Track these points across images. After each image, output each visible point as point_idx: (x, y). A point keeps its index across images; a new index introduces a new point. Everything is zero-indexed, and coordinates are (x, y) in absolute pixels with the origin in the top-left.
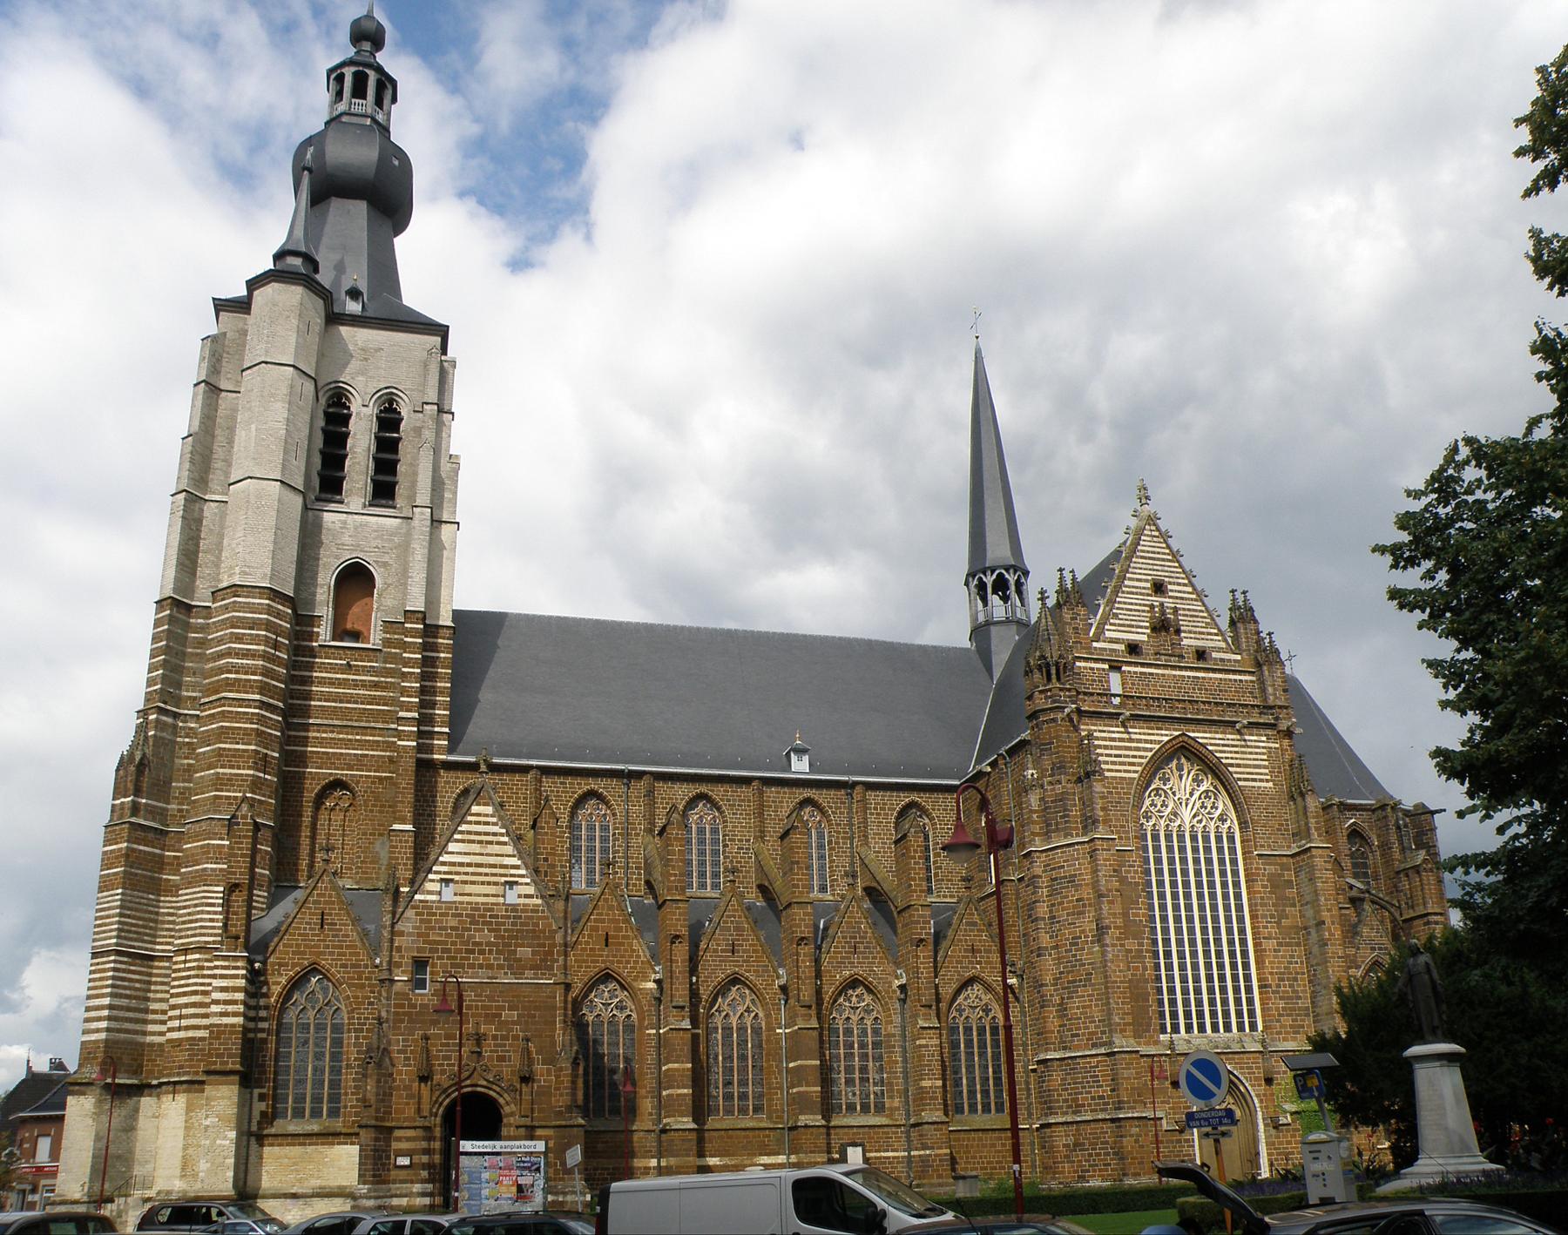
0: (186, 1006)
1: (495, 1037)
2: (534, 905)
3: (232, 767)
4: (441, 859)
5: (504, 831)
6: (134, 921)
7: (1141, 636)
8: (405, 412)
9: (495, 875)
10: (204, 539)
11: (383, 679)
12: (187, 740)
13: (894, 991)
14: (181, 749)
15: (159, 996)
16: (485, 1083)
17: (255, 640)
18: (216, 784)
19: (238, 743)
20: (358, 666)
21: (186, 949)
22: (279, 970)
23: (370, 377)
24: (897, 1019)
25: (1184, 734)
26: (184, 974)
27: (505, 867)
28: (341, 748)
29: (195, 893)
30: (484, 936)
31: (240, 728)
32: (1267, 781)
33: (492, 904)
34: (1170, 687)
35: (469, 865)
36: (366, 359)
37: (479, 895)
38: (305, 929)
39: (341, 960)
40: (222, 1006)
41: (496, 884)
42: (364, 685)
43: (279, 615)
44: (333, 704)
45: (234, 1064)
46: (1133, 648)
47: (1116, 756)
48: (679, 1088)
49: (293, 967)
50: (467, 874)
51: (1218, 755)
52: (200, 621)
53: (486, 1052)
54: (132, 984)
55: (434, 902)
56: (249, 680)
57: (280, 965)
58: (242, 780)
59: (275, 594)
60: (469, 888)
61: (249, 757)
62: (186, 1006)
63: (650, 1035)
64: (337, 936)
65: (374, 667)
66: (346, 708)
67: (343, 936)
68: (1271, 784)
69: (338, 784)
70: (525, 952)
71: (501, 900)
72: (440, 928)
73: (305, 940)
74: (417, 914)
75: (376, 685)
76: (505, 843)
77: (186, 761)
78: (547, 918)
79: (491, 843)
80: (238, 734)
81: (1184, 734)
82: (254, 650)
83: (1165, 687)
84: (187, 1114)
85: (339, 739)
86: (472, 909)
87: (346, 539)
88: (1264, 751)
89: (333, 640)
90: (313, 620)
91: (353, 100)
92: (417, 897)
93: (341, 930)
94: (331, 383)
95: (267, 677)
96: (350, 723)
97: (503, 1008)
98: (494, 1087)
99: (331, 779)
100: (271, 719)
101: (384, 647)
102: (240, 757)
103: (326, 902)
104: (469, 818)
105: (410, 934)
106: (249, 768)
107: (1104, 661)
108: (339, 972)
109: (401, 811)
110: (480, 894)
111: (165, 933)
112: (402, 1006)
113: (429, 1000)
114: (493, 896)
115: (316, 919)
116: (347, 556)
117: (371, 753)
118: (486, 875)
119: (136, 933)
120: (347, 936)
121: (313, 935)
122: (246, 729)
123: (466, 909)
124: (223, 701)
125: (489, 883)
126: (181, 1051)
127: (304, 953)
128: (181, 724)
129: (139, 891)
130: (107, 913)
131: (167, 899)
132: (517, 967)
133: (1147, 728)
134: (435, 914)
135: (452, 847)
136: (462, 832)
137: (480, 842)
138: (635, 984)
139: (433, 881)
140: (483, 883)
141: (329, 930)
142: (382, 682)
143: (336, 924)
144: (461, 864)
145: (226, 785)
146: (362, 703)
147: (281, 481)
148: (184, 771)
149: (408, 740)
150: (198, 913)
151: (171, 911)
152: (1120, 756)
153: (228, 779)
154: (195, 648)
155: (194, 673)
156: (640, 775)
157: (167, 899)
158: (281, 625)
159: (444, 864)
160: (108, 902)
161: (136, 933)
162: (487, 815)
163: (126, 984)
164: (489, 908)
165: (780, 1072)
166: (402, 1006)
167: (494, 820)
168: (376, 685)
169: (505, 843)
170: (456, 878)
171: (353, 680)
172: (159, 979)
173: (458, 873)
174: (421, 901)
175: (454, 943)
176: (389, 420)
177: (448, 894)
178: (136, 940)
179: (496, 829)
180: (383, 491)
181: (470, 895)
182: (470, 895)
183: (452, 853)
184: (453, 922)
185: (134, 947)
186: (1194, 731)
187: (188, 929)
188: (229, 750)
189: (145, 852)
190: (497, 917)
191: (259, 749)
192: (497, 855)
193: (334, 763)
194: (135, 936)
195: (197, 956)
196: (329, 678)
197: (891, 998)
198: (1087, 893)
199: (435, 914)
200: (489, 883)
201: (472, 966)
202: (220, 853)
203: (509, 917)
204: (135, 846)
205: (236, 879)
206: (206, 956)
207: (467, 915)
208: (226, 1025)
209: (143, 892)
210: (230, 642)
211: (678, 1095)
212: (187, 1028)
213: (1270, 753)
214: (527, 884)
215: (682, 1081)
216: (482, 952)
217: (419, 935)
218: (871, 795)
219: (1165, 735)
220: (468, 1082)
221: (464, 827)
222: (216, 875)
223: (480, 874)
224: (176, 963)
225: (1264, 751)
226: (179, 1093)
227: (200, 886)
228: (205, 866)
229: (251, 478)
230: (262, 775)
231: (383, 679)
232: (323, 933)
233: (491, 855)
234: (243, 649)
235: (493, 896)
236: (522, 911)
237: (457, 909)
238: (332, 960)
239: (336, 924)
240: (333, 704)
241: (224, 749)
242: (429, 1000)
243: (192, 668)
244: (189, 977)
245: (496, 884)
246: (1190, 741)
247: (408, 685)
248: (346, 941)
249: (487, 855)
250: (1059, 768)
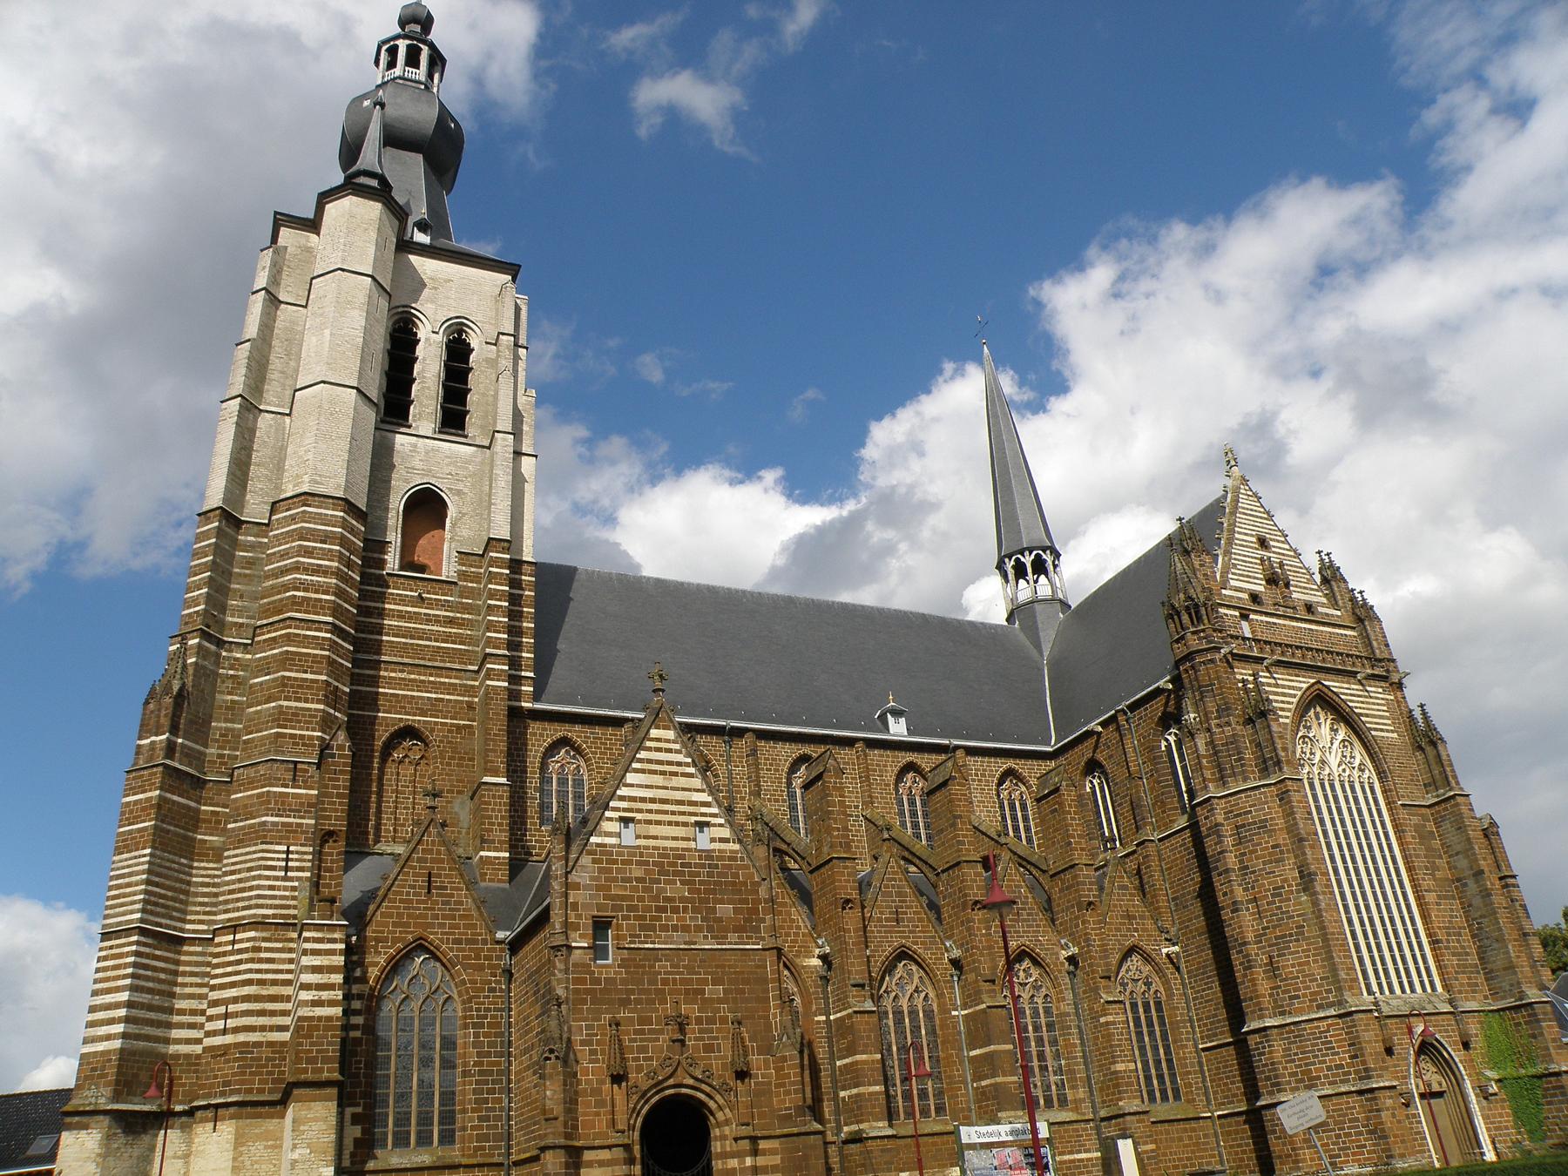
0: (235, 1000)
1: (699, 1021)
2: (731, 851)
3: (298, 700)
4: (619, 792)
5: (689, 760)
6: (163, 892)
7: (1260, 587)
8: (474, 341)
9: (683, 813)
10: (257, 451)
11: (459, 615)
12: (231, 672)
13: (1062, 964)
14: (223, 682)
15: (188, 990)
16: (691, 1082)
17: (327, 555)
18: (279, 719)
19: (306, 672)
20: (431, 599)
21: (235, 927)
22: (376, 947)
23: (440, 306)
24: (1069, 995)
25: (1318, 682)
26: (232, 958)
28: (413, 690)
29: (247, 854)
30: (676, 889)
31: (308, 655)
32: (1392, 731)
33: (683, 849)
35: (653, 801)
36: (436, 288)
37: (666, 838)
38: (408, 894)
39: (454, 934)
40: (314, 992)
41: (685, 824)
42: (437, 620)
43: (352, 530)
44: (403, 640)
45: (330, 1072)
46: (1255, 597)
48: (870, 1085)
49: (394, 943)
50: (650, 811)
51: (1350, 704)
52: (249, 538)
53: (690, 1040)
54: (155, 974)
55: (613, 846)
56: (320, 600)
57: (378, 940)
58: (310, 716)
59: (350, 507)
60: (654, 830)
61: (319, 689)
62: (235, 1000)
63: (819, 1022)
64: (448, 903)
65: (449, 601)
66: (417, 645)
67: (456, 903)
68: (1395, 735)
69: (409, 732)
70: (725, 910)
72: (624, 880)
73: (409, 908)
74: (594, 861)
75: (451, 622)
76: (690, 775)
77: (229, 697)
78: (747, 867)
79: (675, 774)
80: (306, 661)
82: (326, 566)
84: (235, 1149)
85: (410, 680)
86: (660, 855)
87: (417, 463)
88: (1383, 702)
90: (382, 546)
91: (407, 68)
92: (593, 839)
93: (452, 896)
94: (398, 307)
95: (339, 598)
96: (422, 662)
97: (705, 981)
98: (704, 1087)
99: (402, 725)
100: (342, 647)
101: (460, 580)
102: (308, 687)
103: (433, 861)
104: (648, 744)
105: (586, 887)
106: (319, 702)
107: (1235, 608)
108: (451, 950)
109: (492, 762)
110: (668, 836)
111: (198, 909)
112: (583, 981)
113: (615, 973)
114: (683, 839)
115: (421, 882)
116: (418, 480)
117: (448, 697)
118: (673, 813)
119: (163, 906)
120: (461, 903)
121: (418, 902)
122: (315, 656)
123: (652, 855)
124: (288, 623)
125: (677, 824)
126: (227, 1061)
127: (407, 925)
128: (224, 654)
129: (169, 853)
130: (127, 880)
131: (202, 865)
132: (717, 928)
134: (615, 862)
135: (631, 778)
136: (641, 761)
137: (663, 773)
138: (798, 961)
139: (610, 819)
140: (670, 823)
141: (438, 895)
142: (458, 618)
143: (446, 888)
144: (643, 800)
145: (291, 720)
146: (436, 641)
147: (357, 389)
148: (227, 708)
149: (498, 680)
150: (254, 878)
151: (207, 880)
153: (293, 714)
154: (243, 568)
155: (241, 597)
156: (740, 733)
157: (202, 865)
158: (354, 543)
159: (622, 798)
160: (129, 866)
161: (163, 906)
162: (668, 741)
163: (149, 973)
164: (679, 855)
165: (961, 1062)
166: (583, 981)
167: (677, 747)
168: (451, 622)
169: (690, 775)
170: (639, 816)
171: (425, 614)
172: (188, 969)
173: (639, 811)
174: (598, 845)
175: (641, 899)
176: (457, 351)
177: (629, 837)
178: (163, 916)
179: (680, 758)
180: (453, 419)
181: (655, 838)
182: (655, 838)
183: (632, 785)
184: (638, 872)
185: (160, 925)
187: (238, 900)
188: (296, 679)
189: (179, 803)
190: (689, 865)
191: (330, 680)
193: (404, 708)
194: (162, 910)
195: (252, 934)
196: (398, 611)
197: (1060, 971)
198: (1283, 838)
199: (615, 862)
200: (677, 824)
201: (665, 928)
202: (283, 803)
203: (703, 866)
204: (169, 795)
205: (329, 825)
206: (264, 934)
207: (655, 863)
208: (320, 1018)
209: (175, 854)
210: (297, 556)
211: (871, 1094)
212: (236, 1030)
213: (1388, 704)
214: (721, 825)
215: (872, 1076)
216: (675, 910)
217: (598, 888)
218: (970, 760)
219: (1303, 682)
220: (671, 1082)
221: (642, 755)
222: (278, 831)
223: (666, 812)
224: (220, 944)
225: (1383, 702)
226: (223, 1119)
227: (256, 844)
228: (264, 819)
229: (324, 382)
230: (332, 711)
231: (459, 615)
232: (430, 899)
233: (677, 789)
234: (313, 564)
235: (683, 839)
237: (641, 855)
238: (442, 934)
239: (446, 888)
240: (403, 640)
241: (289, 678)
242: (615, 973)
243: (239, 590)
244: (239, 962)
245: (685, 824)
246: (1326, 690)
247: (496, 619)
248: (459, 910)
249: (673, 789)
250: (1224, 710)
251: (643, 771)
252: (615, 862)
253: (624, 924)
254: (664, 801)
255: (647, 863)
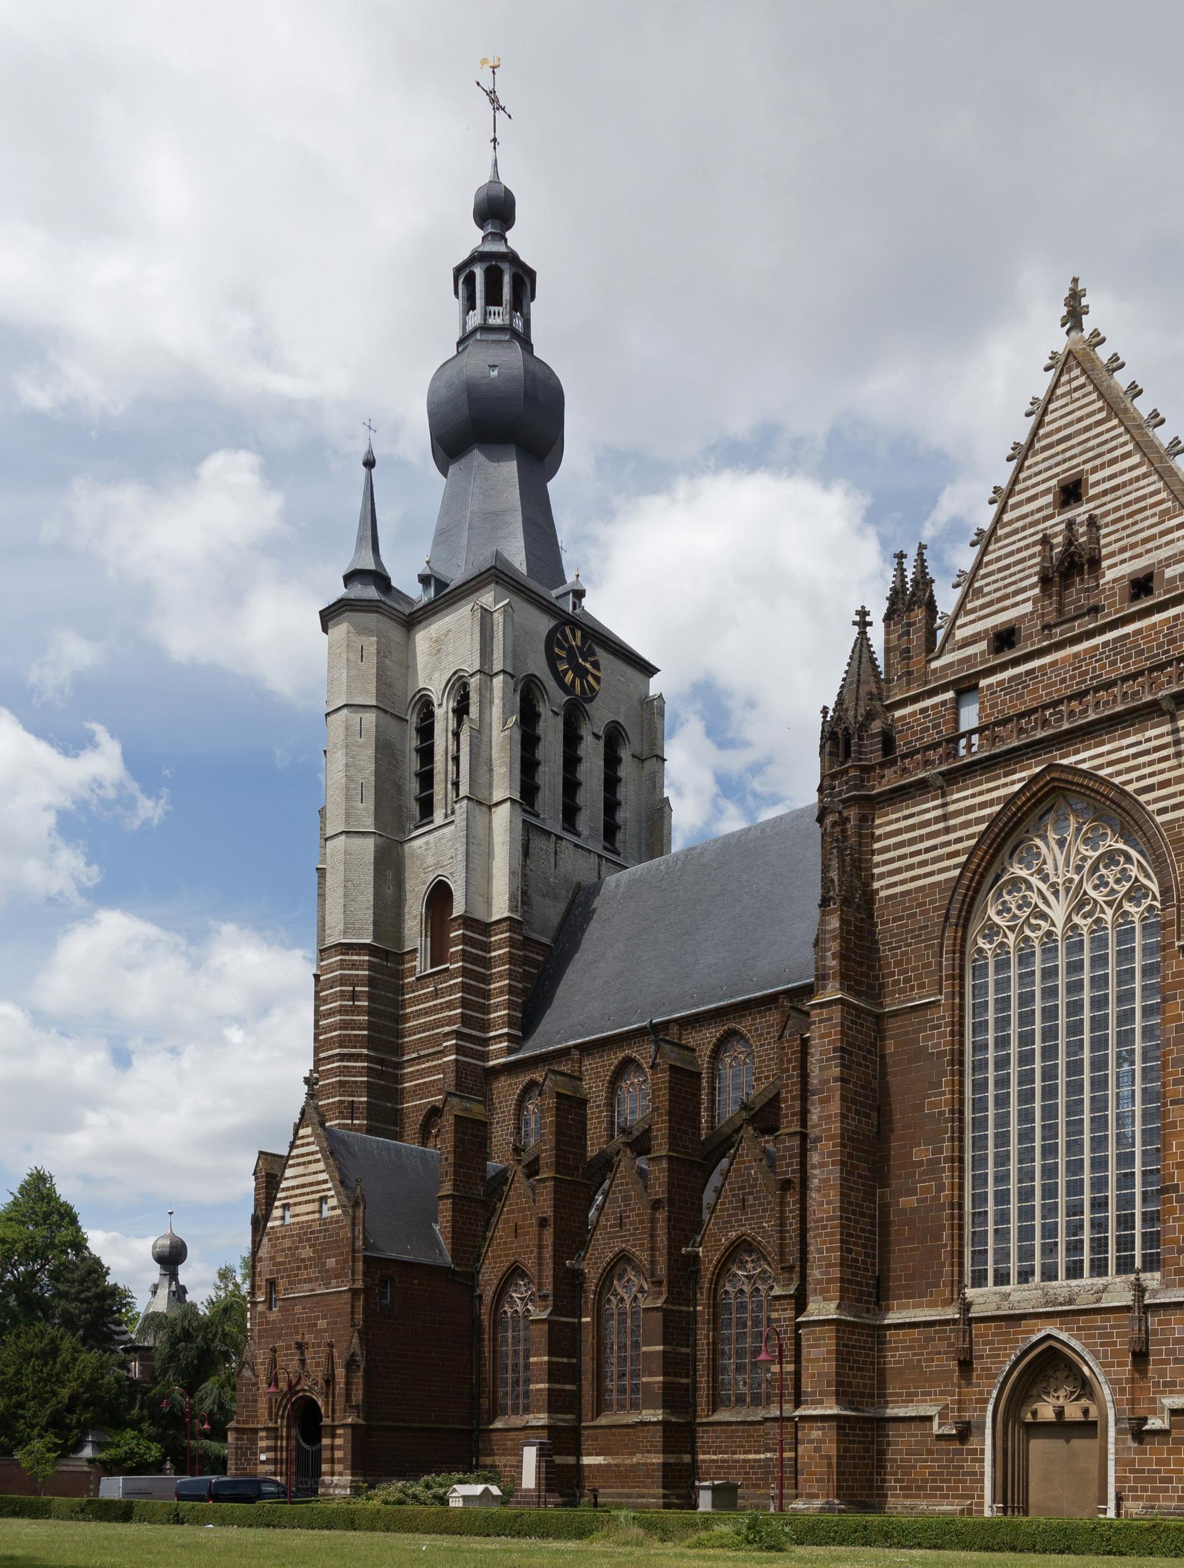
25: (1051, 767)
27: (318, 1183)
30: (306, 1252)
34: (1063, 681)
35: (298, 1187)
37: (303, 1214)
43: (354, 965)
46: (1004, 638)
47: (927, 850)
71: (317, 1216)
74: (270, 1240)
79: (310, 1162)
81: (1051, 767)
83: (1054, 684)
89: (432, 967)
92: (270, 1224)
100: (355, 1067)
107: (944, 688)
133: (988, 781)
147: (346, 832)
152: (934, 848)
158: (357, 975)
159: (283, 1190)
170: (291, 1201)
173: (291, 1197)
184: (287, 1243)
186: (1077, 752)
192: (315, 1173)
236: (331, 1223)
245: (313, 1201)
249: (309, 1174)
251: (299, 1164)
252: (278, 1238)
253: (282, 1283)
254: (303, 1186)
255: (292, 1236)
